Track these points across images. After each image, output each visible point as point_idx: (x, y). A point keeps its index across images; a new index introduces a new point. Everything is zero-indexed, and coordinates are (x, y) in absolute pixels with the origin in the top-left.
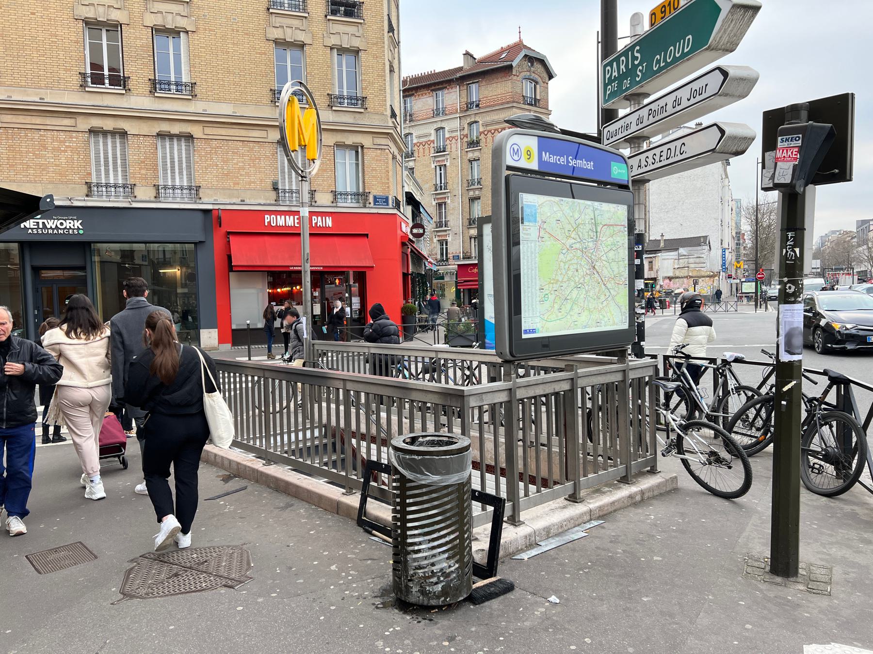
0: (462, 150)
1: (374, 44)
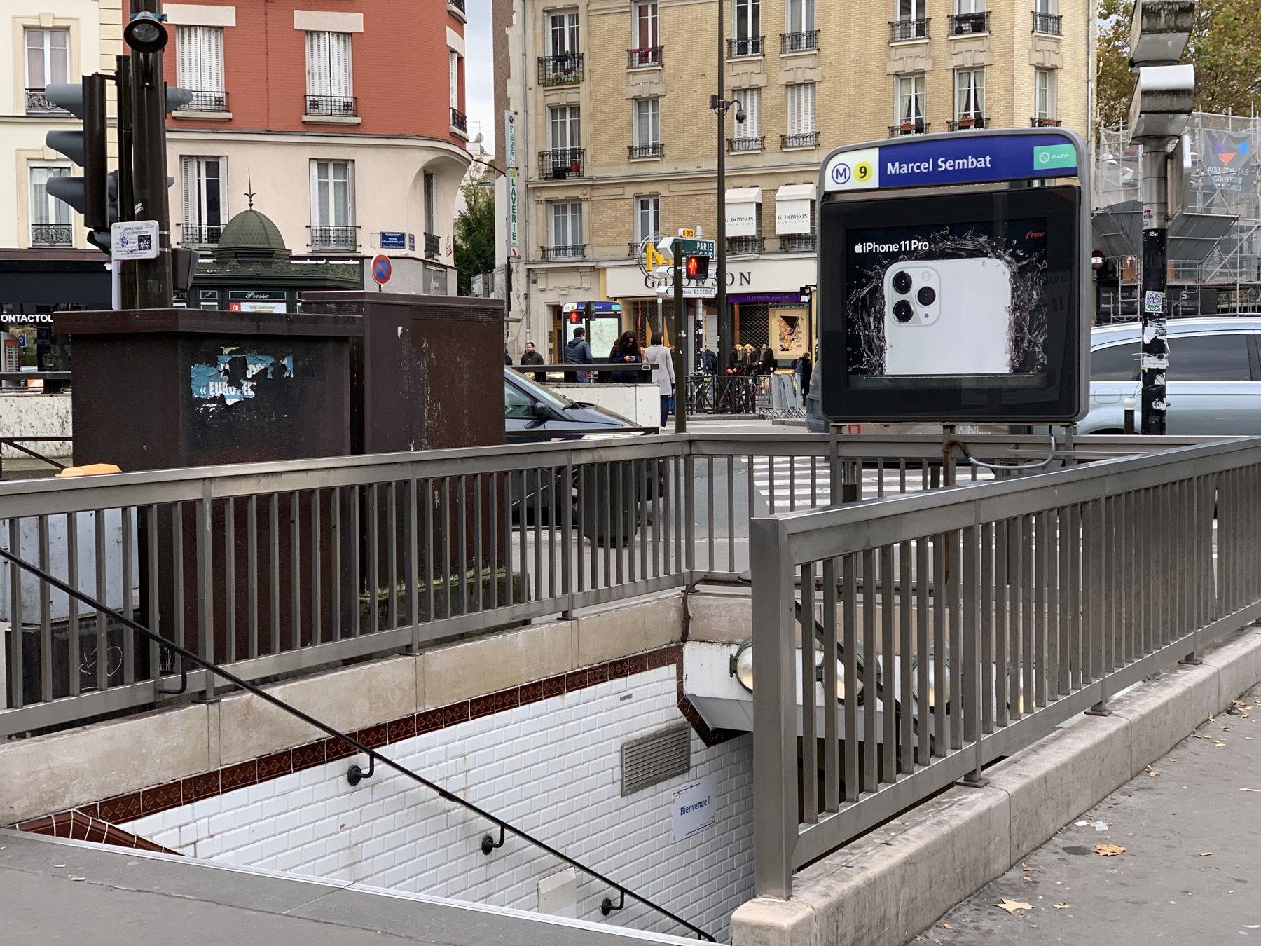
1: (1000, 56)
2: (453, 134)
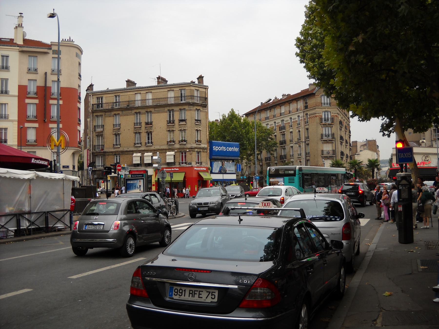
0: (304, 125)
2: (78, 146)
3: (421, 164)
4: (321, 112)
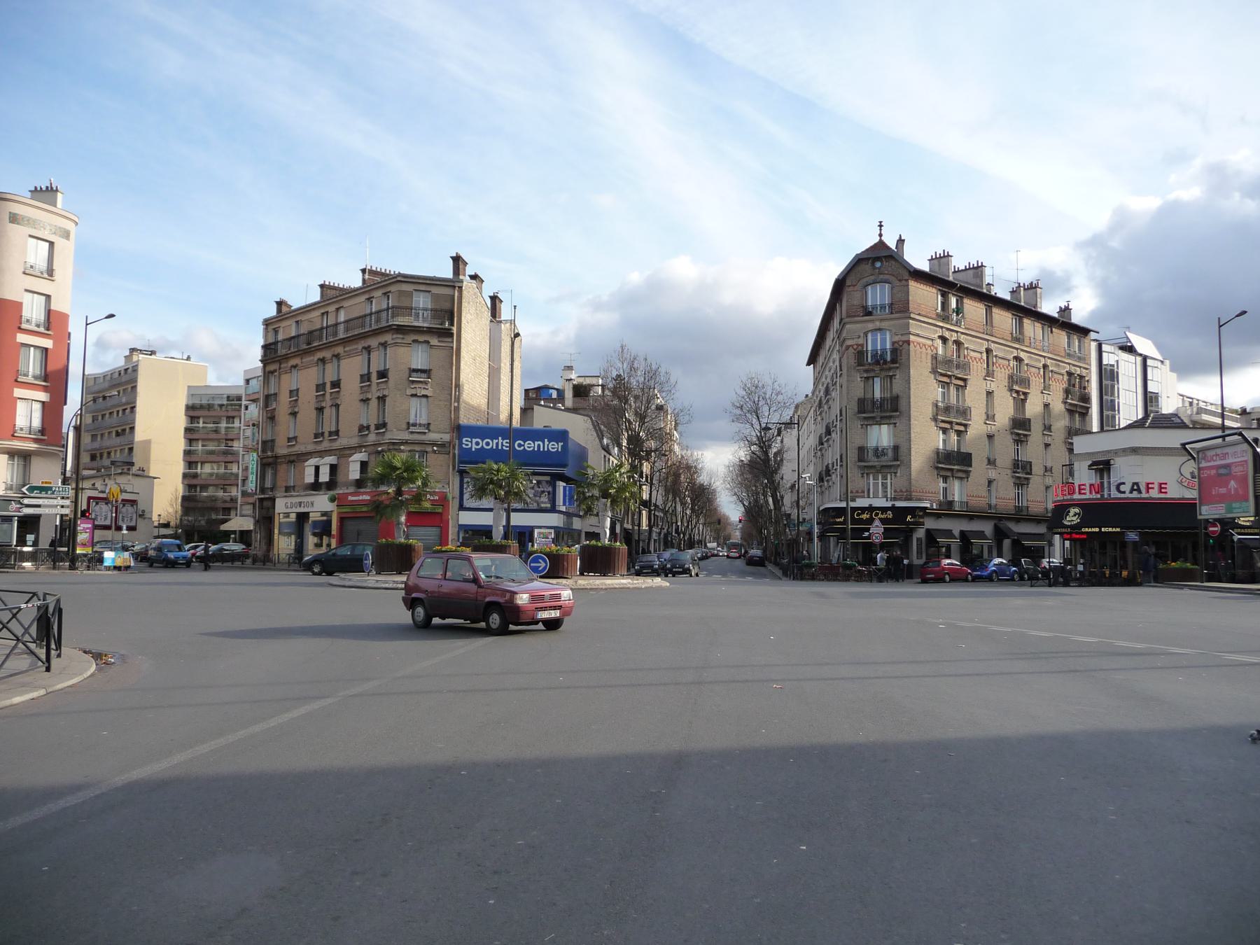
3: (1148, 489)
4: (862, 335)
